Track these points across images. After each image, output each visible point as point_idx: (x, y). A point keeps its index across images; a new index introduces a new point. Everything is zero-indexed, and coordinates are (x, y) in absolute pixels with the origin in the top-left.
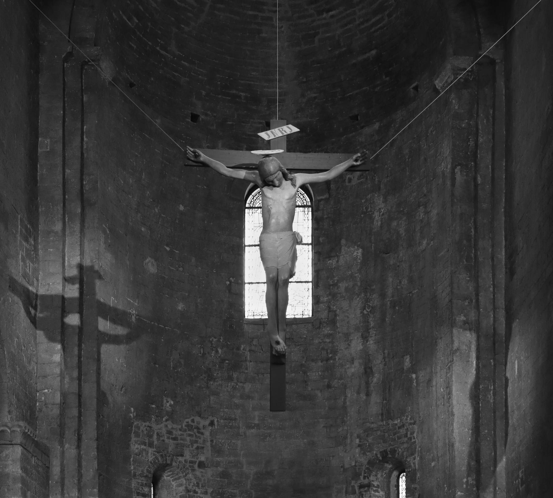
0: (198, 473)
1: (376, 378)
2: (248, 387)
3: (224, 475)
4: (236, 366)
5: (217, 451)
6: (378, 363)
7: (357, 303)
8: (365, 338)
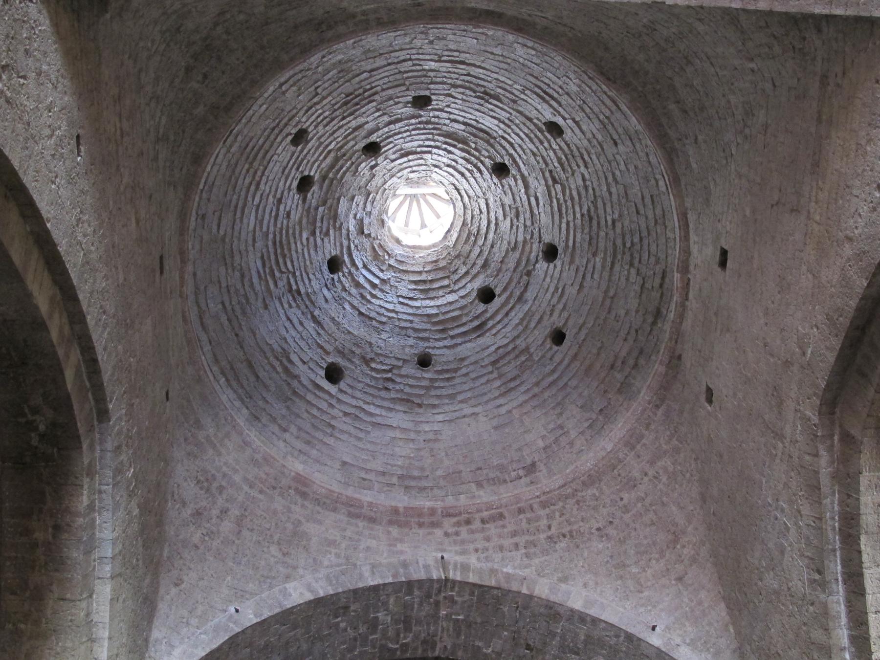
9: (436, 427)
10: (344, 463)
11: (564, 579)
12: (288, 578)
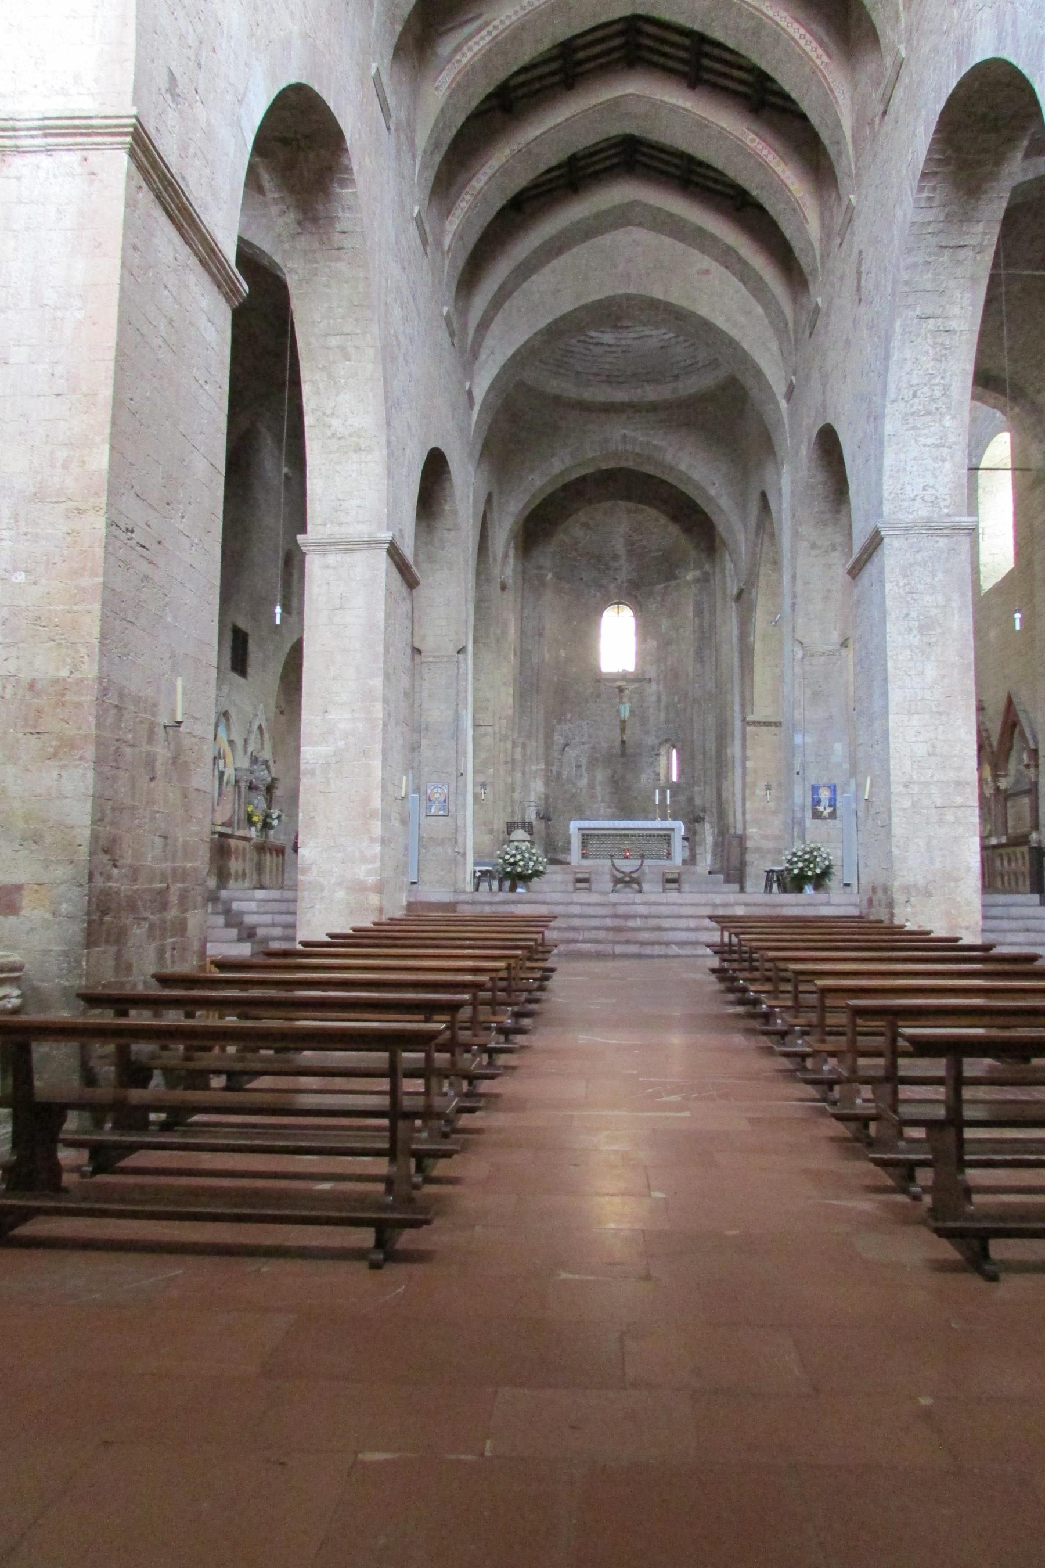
0: (582, 747)
1: (663, 705)
2: (604, 706)
3: (593, 748)
4: (598, 696)
5: (590, 736)
6: (664, 698)
8: (658, 684)
9: (629, 342)
10: (578, 372)
11: (681, 449)
12: (553, 455)
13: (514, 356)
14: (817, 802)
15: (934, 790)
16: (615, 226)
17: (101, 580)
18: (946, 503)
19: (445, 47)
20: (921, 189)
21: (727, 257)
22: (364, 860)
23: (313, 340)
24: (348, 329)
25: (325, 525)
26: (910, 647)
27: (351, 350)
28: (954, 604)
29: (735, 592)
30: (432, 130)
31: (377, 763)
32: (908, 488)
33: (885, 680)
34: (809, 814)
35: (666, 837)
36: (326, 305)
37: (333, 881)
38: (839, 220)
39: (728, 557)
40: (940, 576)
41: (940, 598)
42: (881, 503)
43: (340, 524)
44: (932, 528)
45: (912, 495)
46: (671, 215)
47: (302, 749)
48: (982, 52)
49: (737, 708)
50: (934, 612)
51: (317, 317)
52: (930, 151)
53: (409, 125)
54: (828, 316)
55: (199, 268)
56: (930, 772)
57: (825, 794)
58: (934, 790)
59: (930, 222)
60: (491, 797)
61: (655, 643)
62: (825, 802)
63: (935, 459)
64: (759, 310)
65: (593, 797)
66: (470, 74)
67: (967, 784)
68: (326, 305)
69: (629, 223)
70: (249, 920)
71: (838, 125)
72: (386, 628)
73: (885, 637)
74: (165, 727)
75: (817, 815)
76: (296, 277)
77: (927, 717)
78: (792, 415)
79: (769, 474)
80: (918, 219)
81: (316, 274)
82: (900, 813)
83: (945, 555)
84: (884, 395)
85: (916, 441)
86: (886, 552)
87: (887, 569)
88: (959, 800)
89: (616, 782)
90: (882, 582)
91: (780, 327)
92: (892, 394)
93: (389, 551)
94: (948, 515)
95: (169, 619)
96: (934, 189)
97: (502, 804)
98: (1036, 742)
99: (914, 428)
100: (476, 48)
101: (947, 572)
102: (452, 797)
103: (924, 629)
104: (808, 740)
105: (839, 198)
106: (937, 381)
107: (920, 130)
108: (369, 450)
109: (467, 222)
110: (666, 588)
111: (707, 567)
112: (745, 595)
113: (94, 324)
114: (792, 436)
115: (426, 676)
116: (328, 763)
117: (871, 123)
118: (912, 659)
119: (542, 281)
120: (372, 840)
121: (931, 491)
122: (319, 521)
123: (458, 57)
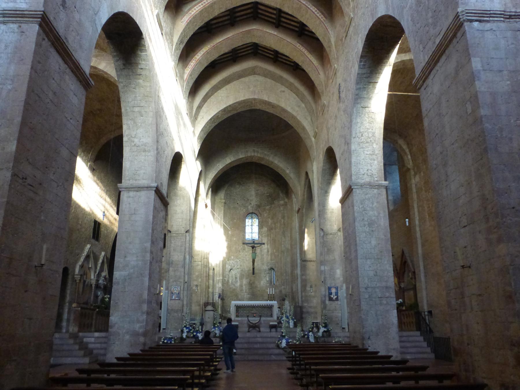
1: (270, 253)
3: (242, 270)
5: (241, 266)
7: (266, 238)
8: (268, 245)
13: (211, 119)
14: (330, 294)
15: (377, 290)
16: (250, 74)
17: (5, 200)
18: (376, 176)
19: (186, 9)
20: (361, 61)
21: (291, 87)
22: (138, 321)
23: (128, 108)
24: (142, 105)
25: (129, 180)
26: (365, 232)
27: (143, 113)
28: (381, 215)
29: (297, 209)
30: (180, 37)
31: (146, 279)
32: (361, 170)
33: (356, 245)
34: (327, 298)
35: (271, 307)
36: (134, 96)
37: (124, 331)
38: (331, 74)
39: (293, 196)
40: (375, 204)
41: (376, 213)
42: (351, 176)
43: (136, 180)
44: (371, 186)
45: (363, 173)
46: (270, 71)
47: (114, 273)
48: (381, 12)
49: (298, 255)
50: (373, 218)
51: (130, 100)
52: (363, 48)
53: (170, 34)
54: (328, 107)
55: (71, 74)
56: (375, 283)
57: (333, 291)
58: (377, 290)
59: (364, 74)
60: (200, 291)
61: (266, 229)
62: (334, 294)
63: (371, 160)
64: (303, 105)
65: (242, 290)
66: (195, 17)
67: (391, 288)
68: (134, 96)
69: (255, 73)
70: (91, 346)
71: (329, 41)
72: (153, 222)
73: (355, 228)
74: (36, 266)
75: (331, 299)
76: (122, 85)
77: (373, 260)
78: (317, 143)
79: (309, 165)
80: (360, 72)
81: (130, 84)
82: (364, 300)
83: (377, 196)
84: (351, 135)
85: (364, 153)
86: (354, 194)
87: (355, 201)
88: (387, 294)
89: (251, 284)
90: (353, 206)
91: (311, 112)
92: (354, 136)
93: (155, 191)
94: (377, 181)
95: (42, 218)
96: (365, 62)
97: (204, 294)
98: (414, 269)
99: (363, 148)
100: (197, 9)
101: (377, 202)
102: (182, 292)
103: (370, 225)
104: (326, 268)
105: (331, 66)
106: (370, 131)
107: (360, 41)
108: (149, 151)
109: (193, 70)
110: (271, 207)
111: (286, 200)
112: (301, 210)
113: (16, 91)
114: (317, 152)
115: (173, 241)
116: (125, 279)
117: (342, 40)
118: (366, 237)
119: (222, 93)
120: (143, 313)
121: (370, 171)
122: (127, 178)
123: (190, 12)
